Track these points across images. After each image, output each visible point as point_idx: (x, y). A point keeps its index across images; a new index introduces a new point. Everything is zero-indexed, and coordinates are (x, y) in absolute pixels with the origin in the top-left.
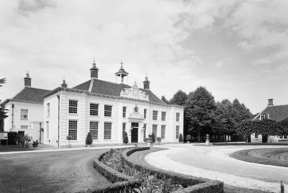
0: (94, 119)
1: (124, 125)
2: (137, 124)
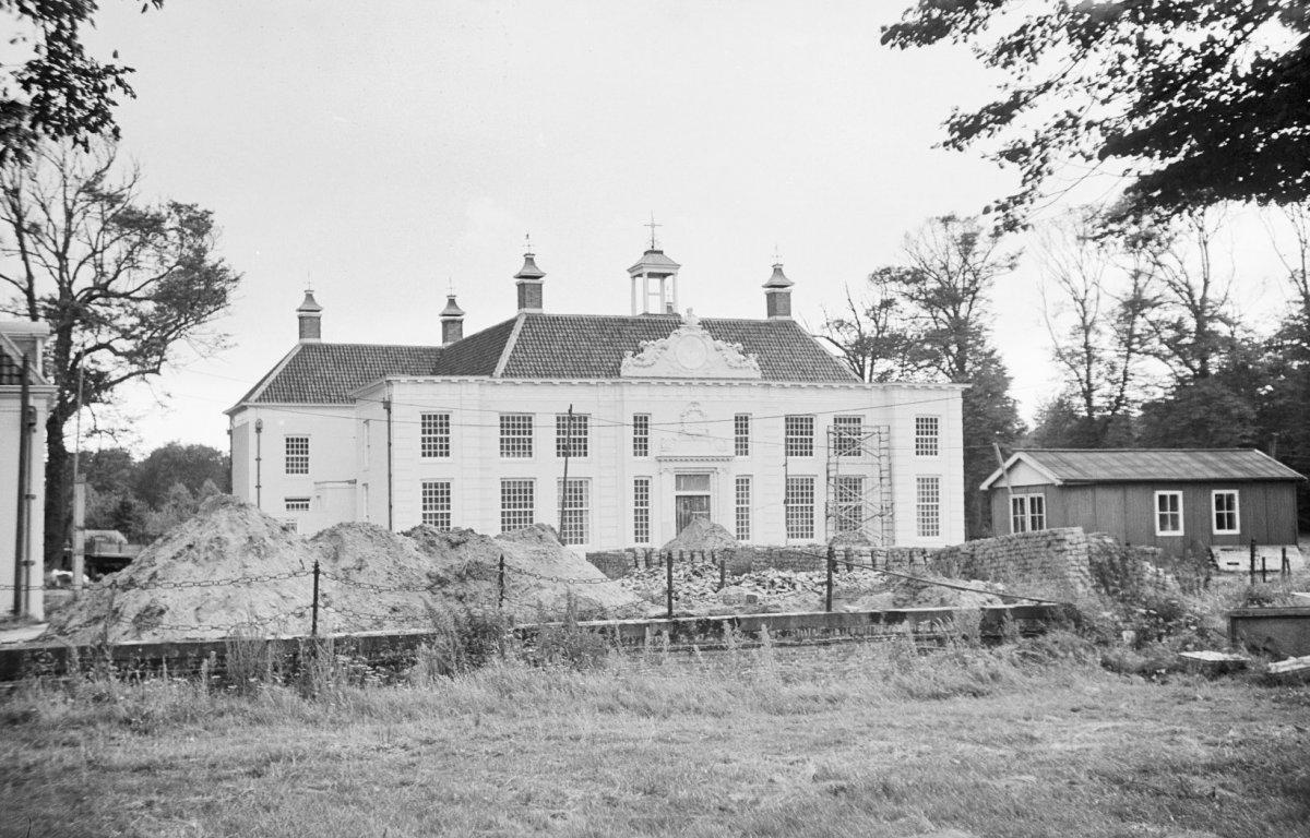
0: (517, 468)
1: (642, 487)
2: (703, 479)
